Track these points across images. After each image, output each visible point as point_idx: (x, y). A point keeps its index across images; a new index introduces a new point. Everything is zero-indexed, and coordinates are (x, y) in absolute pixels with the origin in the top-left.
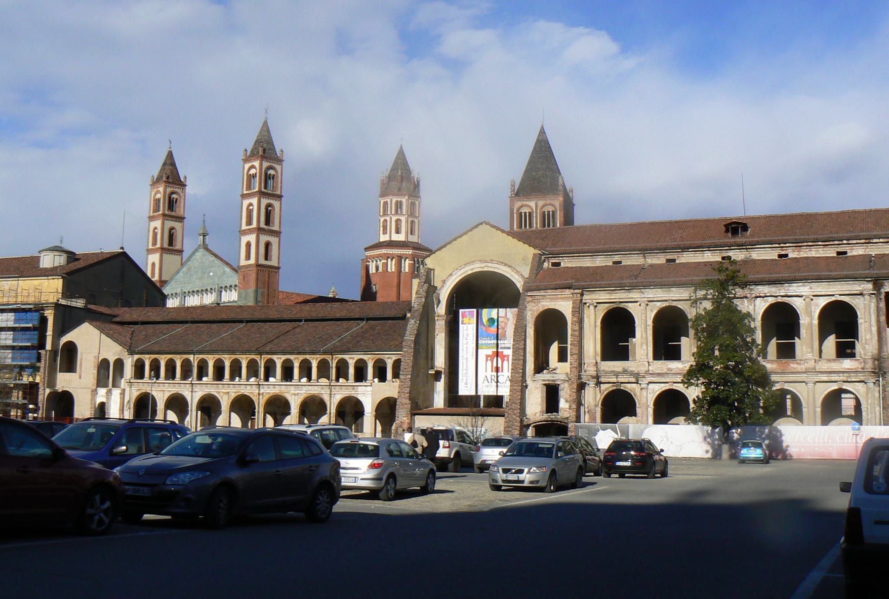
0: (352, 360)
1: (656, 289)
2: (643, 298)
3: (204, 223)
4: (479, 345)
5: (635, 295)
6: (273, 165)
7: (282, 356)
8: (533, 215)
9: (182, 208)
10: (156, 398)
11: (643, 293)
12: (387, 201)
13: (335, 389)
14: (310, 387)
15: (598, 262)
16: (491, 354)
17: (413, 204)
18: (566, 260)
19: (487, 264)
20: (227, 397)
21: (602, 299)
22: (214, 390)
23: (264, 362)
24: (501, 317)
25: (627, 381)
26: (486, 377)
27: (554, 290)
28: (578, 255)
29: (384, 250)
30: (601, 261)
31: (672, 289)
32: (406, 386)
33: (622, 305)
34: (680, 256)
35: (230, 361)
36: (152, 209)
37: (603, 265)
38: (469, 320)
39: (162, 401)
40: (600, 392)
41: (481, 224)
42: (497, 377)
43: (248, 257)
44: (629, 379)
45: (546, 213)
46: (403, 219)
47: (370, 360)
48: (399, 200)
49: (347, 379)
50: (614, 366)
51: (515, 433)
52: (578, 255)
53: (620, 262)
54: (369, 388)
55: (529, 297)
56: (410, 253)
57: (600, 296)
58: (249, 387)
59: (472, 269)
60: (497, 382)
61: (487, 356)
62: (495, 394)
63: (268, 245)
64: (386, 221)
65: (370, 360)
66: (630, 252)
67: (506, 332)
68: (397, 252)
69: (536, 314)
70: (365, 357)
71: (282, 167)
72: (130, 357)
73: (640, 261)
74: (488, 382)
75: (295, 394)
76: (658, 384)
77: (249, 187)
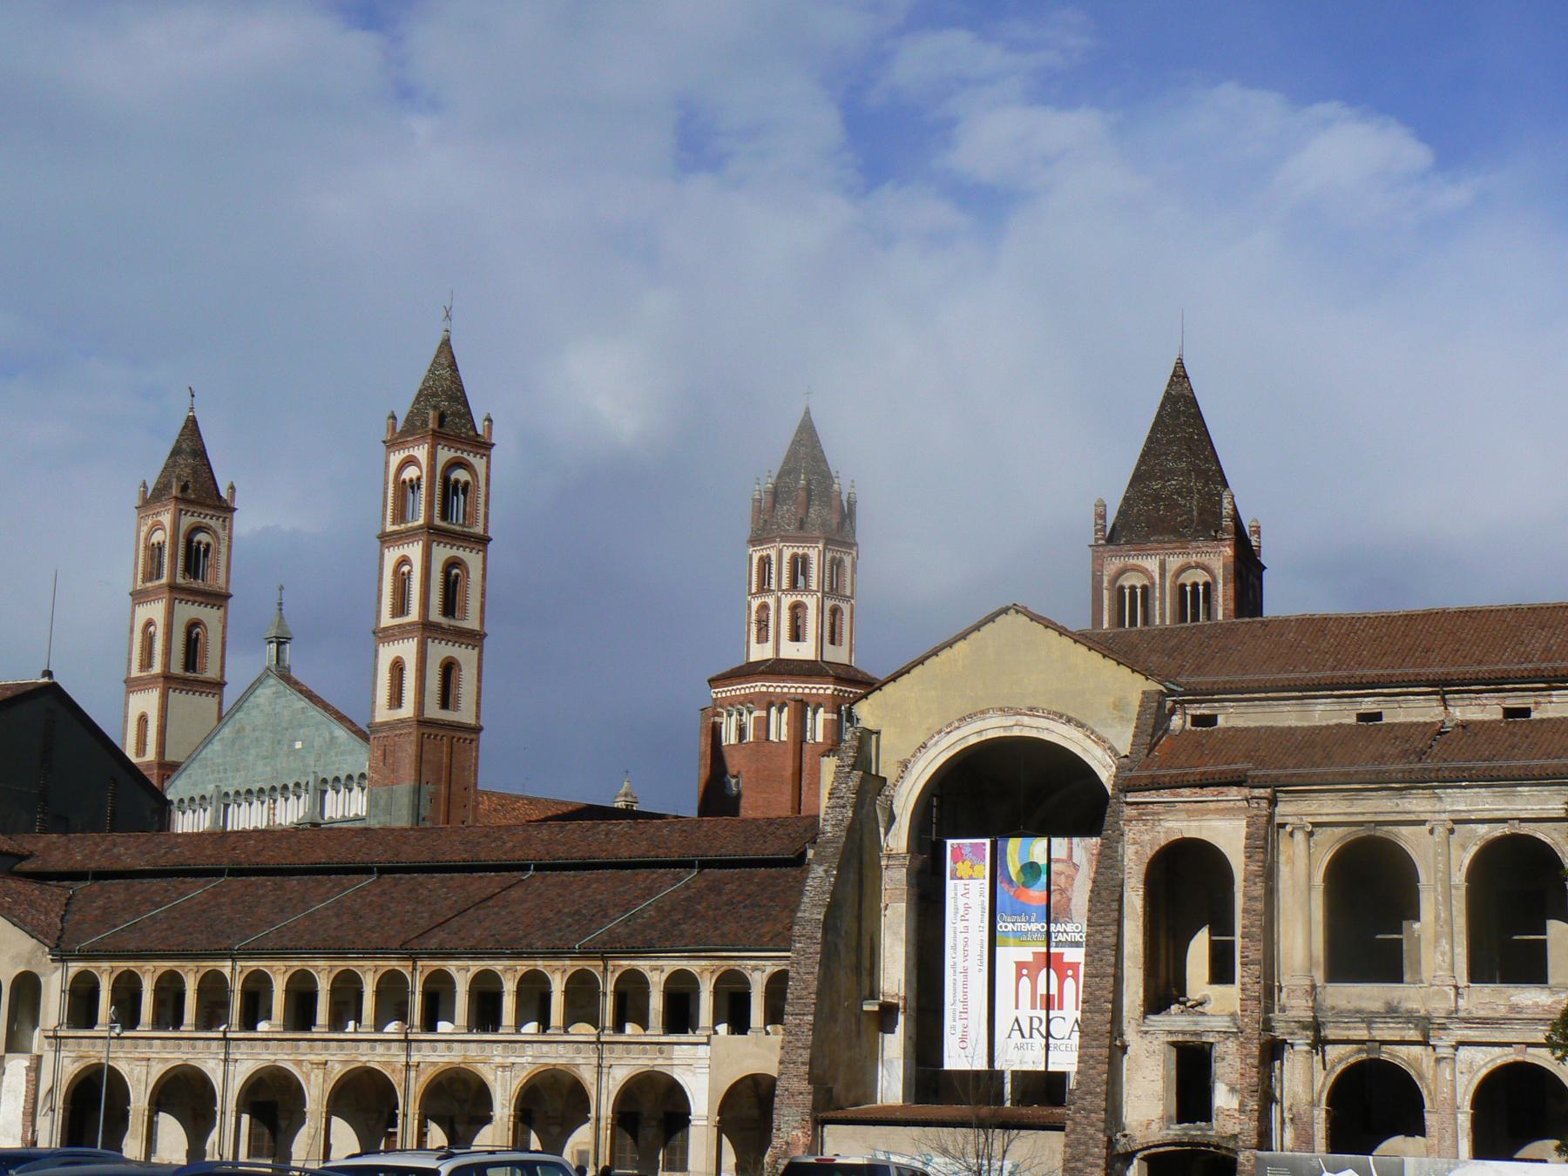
0: (657, 972)
1: (1477, 790)
2: (1439, 812)
3: (281, 610)
4: (998, 934)
5: (1416, 803)
6: (465, 455)
7: (470, 963)
8: (1154, 592)
9: (223, 569)
10: (127, 1080)
11: (1440, 798)
12: (768, 557)
14: (545, 1048)
16: (1030, 958)
17: (837, 564)
19: (1018, 717)
20: (321, 1076)
21: (1327, 814)
22: (286, 1057)
23: (423, 978)
24: (1058, 861)
25: (1398, 1039)
26: (1017, 1020)
27: (1197, 790)
29: (759, 684)
30: (1326, 713)
31: (1519, 789)
33: (1381, 832)
34: (1540, 699)
35: (332, 976)
37: (1333, 722)
38: (972, 867)
39: (143, 1088)
40: (1325, 1068)
41: (1005, 611)
42: (1048, 1021)
43: (396, 700)
44: (1403, 1033)
45: (1188, 589)
46: (811, 602)
48: (800, 551)
49: (645, 1026)
50: (1360, 997)
52: (1263, 695)
54: (703, 1051)
55: (1129, 808)
56: (829, 692)
57: (1322, 806)
58: (380, 1048)
60: (1048, 1034)
61: (1020, 966)
62: (1042, 1068)
63: (449, 669)
64: (764, 607)
65: (706, 973)
66: (1405, 690)
67: (1070, 900)
68: (793, 690)
69: (1149, 853)
70: (693, 966)
71: (488, 462)
72: (57, 968)
73: (1432, 714)
74: (1023, 1037)
75: (504, 1067)
76: (1484, 1048)
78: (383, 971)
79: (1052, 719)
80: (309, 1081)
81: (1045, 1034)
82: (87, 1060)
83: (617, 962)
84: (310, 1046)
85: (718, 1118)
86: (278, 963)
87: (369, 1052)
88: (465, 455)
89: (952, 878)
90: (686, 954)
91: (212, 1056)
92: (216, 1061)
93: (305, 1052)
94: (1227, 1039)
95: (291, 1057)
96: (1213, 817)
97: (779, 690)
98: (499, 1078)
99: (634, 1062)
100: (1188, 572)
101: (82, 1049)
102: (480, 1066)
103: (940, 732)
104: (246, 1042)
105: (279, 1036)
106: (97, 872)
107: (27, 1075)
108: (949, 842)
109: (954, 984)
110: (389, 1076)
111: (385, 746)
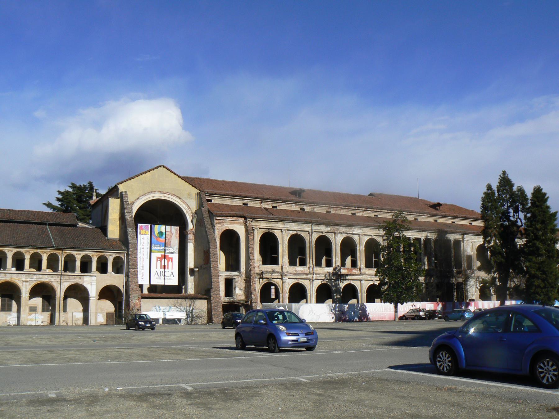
0: (78, 255)
1: (292, 223)
2: (284, 228)
4: (152, 250)
5: (280, 225)
7: (13, 249)
11: (284, 225)
13: (63, 278)
14: (41, 276)
15: (234, 202)
16: (160, 256)
18: (215, 199)
19: (164, 194)
21: (262, 226)
24: (168, 232)
25: (276, 277)
26: (157, 272)
27: (232, 218)
28: (225, 196)
30: (237, 202)
31: (300, 224)
32: (135, 277)
33: (271, 231)
34: (279, 205)
37: (238, 205)
38: (145, 231)
41: (160, 166)
42: (165, 272)
44: (278, 276)
47: (94, 256)
50: (267, 268)
51: (220, 310)
52: (225, 196)
53: (247, 204)
54: (94, 278)
55: (216, 220)
57: (260, 224)
59: (153, 197)
60: (165, 275)
61: (158, 258)
62: (163, 284)
65: (94, 256)
67: (170, 242)
69: (221, 232)
70: (90, 254)
74: (158, 276)
75: (26, 282)
76: (291, 280)
79: (173, 196)
87: (68, 279)
89: (140, 234)
94: (239, 277)
98: (24, 285)
102: (16, 281)
108: (139, 225)
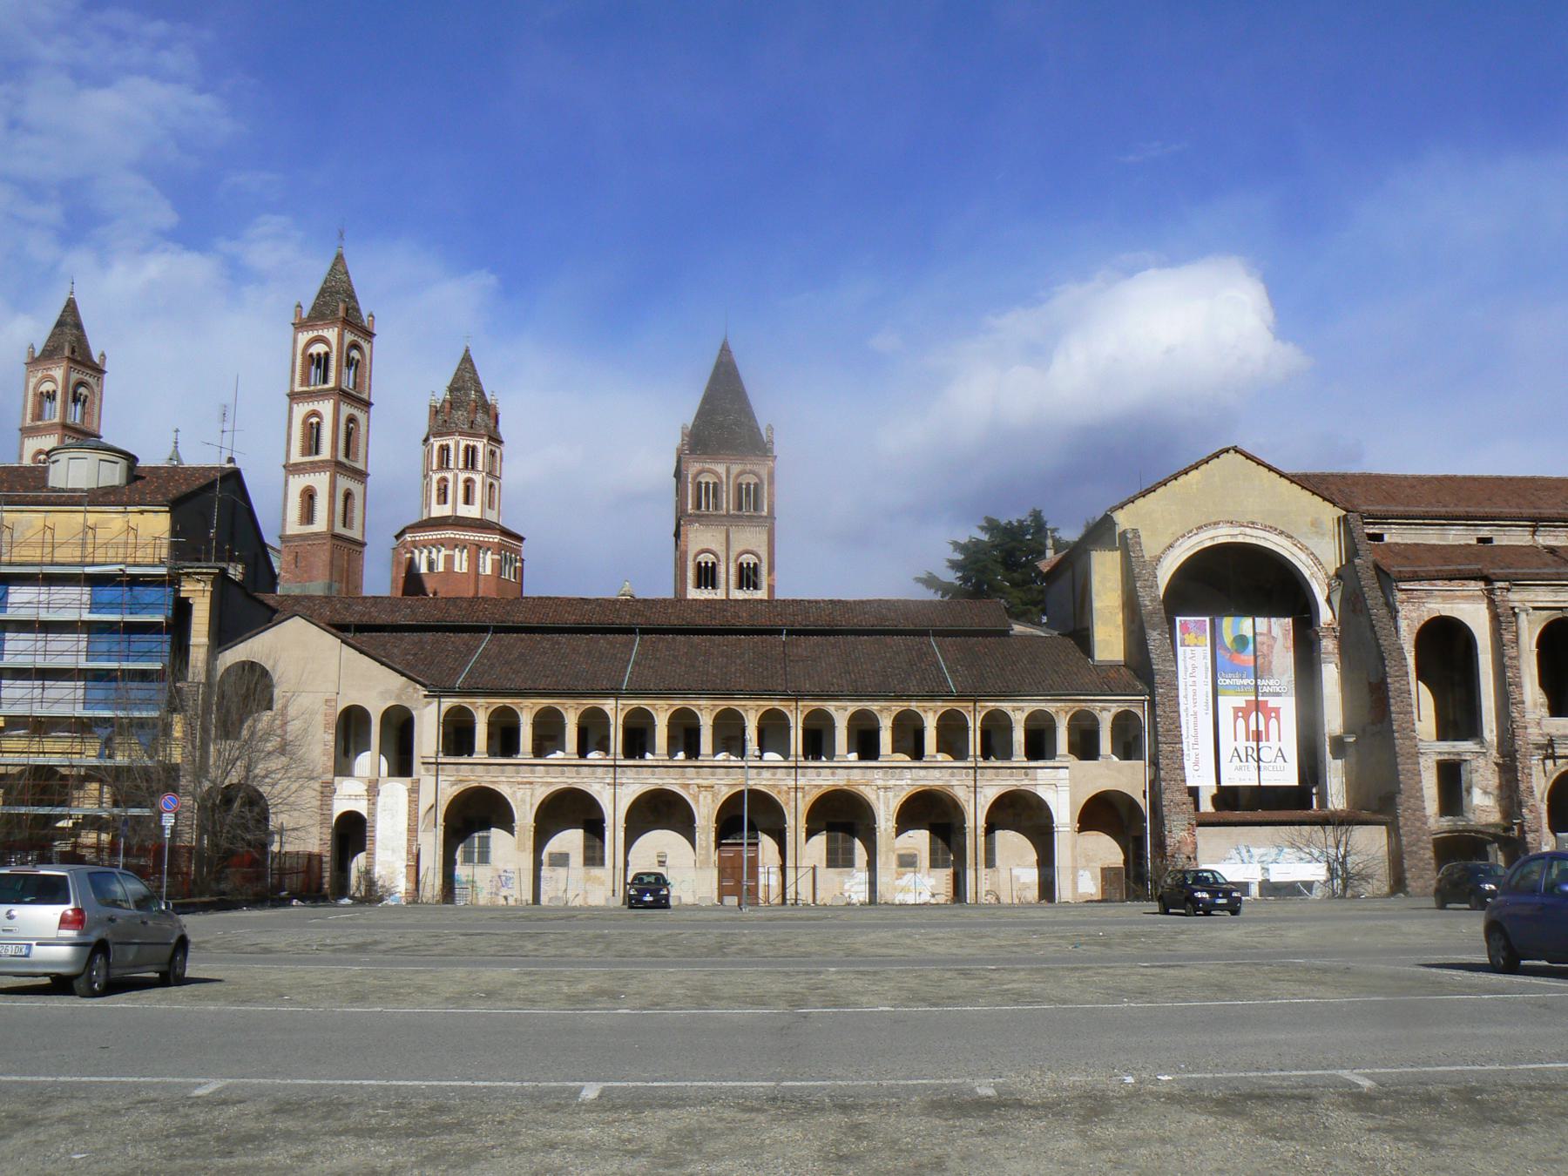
0: (1018, 713)
3: (176, 447)
4: (1219, 687)
6: (359, 340)
7: (849, 704)
8: (722, 488)
9: (96, 417)
10: (510, 800)
12: (448, 446)
14: (922, 772)
15: (1451, 537)
17: (492, 453)
18: (1394, 531)
19: (1242, 528)
20: (710, 797)
21: (1542, 601)
22: (674, 781)
23: (803, 716)
24: (1261, 634)
27: (1446, 582)
28: (1421, 521)
29: (449, 532)
30: (1458, 536)
32: (1177, 766)
35: (714, 714)
36: (29, 411)
37: (1462, 542)
39: (528, 807)
40: (1545, 776)
41: (1227, 451)
42: (1259, 750)
43: (308, 516)
45: (744, 486)
46: (478, 478)
48: (471, 443)
49: (786, 756)
51: (1427, 856)
52: (1421, 521)
53: (1490, 540)
54: (1063, 773)
55: (1401, 593)
56: (496, 540)
57: (1537, 596)
58: (766, 774)
59: (1212, 538)
60: (1259, 759)
61: (1237, 710)
62: (1257, 784)
63: (348, 495)
64: (444, 479)
66: (1513, 523)
67: (1270, 662)
68: (472, 538)
69: (1418, 626)
70: (1050, 707)
71: (372, 347)
72: (429, 703)
73: (1525, 540)
74: (1241, 761)
75: (886, 788)
77: (38, 416)
78: (764, 710)
79: (1268, 531)
80: (697, 802)
81: (1256, 759)
82: (467, 783)
83: (983, 704)
84: (698, 773)
85: (1078, 825)
86: (663, 702)
87: (994, 777)
88: (359, 340)
89: (1181, 646)
90: (1049, 698)
91: (598, 780)
92: (602, 785)
93: (692, 777)
94: (1478, 757)
95: (678, 782)
96: (1462, 601)
97: (462, 537)
98: (881, 798)
99: (1004, 783)
100: (745, 475)
101: (461, 774)
102: (862, 788)
103: (1184, 536)
104: (633, 769)
105: (574, 762)
106: (360, 625)
107: (409, 796)
108: (1178, 619)
109: (1187, 723)
110: (776, 797)
111: (297, 553)
